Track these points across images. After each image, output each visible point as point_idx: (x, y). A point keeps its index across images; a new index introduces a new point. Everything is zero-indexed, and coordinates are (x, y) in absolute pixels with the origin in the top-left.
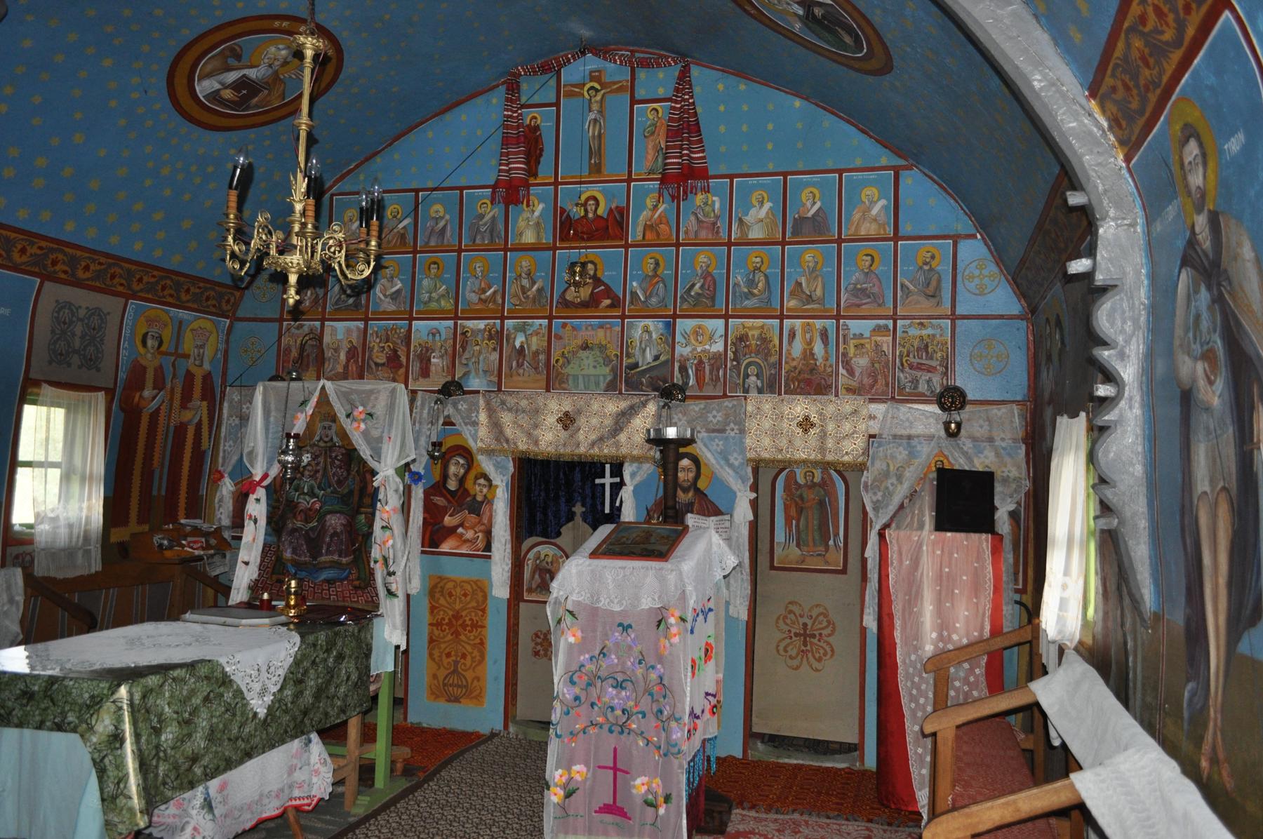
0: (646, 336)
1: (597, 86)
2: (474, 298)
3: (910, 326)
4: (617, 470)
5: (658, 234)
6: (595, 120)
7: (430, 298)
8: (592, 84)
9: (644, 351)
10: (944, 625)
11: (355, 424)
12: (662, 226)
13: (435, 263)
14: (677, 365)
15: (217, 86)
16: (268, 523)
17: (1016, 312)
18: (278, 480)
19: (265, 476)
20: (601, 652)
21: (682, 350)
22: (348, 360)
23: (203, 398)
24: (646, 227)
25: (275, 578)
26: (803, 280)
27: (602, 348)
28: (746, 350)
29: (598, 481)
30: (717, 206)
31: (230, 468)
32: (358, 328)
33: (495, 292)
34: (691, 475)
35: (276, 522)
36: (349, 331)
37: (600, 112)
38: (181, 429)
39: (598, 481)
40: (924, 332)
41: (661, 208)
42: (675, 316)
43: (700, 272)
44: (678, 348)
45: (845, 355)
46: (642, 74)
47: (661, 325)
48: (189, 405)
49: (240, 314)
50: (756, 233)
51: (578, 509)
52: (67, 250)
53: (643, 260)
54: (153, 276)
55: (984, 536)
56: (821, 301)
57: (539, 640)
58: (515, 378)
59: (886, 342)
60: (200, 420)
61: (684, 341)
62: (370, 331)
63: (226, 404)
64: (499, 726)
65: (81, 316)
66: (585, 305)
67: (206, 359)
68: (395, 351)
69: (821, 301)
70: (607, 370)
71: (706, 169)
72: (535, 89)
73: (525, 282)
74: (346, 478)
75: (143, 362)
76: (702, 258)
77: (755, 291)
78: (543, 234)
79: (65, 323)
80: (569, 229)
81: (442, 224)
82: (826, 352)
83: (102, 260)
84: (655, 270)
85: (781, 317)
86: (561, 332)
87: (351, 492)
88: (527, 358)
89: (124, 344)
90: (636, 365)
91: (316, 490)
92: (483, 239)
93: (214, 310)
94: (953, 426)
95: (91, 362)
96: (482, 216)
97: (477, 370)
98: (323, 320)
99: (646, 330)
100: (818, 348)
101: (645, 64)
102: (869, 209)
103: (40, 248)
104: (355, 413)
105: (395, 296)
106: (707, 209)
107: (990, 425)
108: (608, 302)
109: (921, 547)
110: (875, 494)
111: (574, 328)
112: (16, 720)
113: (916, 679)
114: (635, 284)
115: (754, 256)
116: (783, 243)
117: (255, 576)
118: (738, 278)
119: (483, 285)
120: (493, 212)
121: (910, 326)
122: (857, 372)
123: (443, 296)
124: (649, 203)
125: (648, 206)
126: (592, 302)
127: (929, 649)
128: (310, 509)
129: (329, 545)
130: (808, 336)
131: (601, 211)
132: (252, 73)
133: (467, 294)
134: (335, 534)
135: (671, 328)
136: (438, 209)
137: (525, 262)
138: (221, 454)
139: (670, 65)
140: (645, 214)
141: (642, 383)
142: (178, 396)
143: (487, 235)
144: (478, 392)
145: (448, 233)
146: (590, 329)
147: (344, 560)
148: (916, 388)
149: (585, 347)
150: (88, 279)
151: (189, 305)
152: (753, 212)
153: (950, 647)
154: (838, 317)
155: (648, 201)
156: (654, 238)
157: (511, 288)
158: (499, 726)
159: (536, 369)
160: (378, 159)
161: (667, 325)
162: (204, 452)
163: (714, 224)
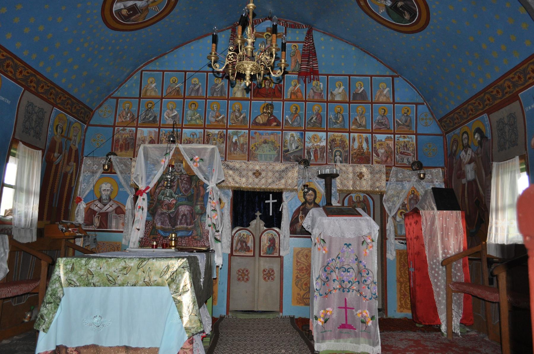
2: (213, 120)
3: (400, 137)
4: (278, 195)
5: (297, 96)
7: (191, 119)
9: (292, 145)
10: (445, 248)
11: (195, 164)
13: (194, 104)
15: (122, 7)
16: (148, 211)
17: (439, 133)
19: (147, 188)
20: (337, 257)
21: (308, 145)
24: (291, 93)
25: (152, 236)
26: (358, 118)
27: (273, 143)
29: (266, 202)
30: (322, 86)
31: (84, 196)
32: (155, 131)
33: (223, 118)
34: (313, 197)
35: (152, 211)
38: (66, 175)
39: (266, 202)
40: (405, 140)
41: (298, 86)
42: (305, 131)
43: (315, 113)
44: (306, 144)
45: (375, 148)
46: (289, 30)
47: (299, 134)
48: (70, 164)
49: (92, 122)
50: (337, 98)
51: (258, 214)
52: (38, 76)
53: (292, 107)
55: (458, 212)
56: (365, 126)
57: (240, 273)
58: (233, 155)
59: (391, 144)
61: (308, 141)
62: (161, 133)
63: (83, 166)
64: (224, 313)
65: (36, 111)
66: (264, 124)
67: (77, 143)
69: (365, 126)
70: (275, 152)
71: (318, 71)
73: (237, 114)
74: (189, 189)
75: (56, 139)
76: (316, 107)
79: (30, 113)
81: (197, 87)
82: (368, 146)
83: (49, 84)
84: (296, 111)
85: (349, 132)
86: (254, 136)
87: (192, 195)
89: (50, 129)
90: (288, 151)
91: (174, 195)
92: (217, 94)
94: (422, 176)
95: (38, 135)
96: (217, 85)
98: (137, 127)
99: (292, 136)
100: (365, 145)
101: (293, 26)
102: (383, 91)
103: (28, 73)
104: (195, 158)
105: (174, 117)
106: (318, 87)
107: (432, 176)
108: (275, 124)
109: (434, 216)
110: (389, 204)
111: (260, 134)
112: (119, 282)
113: (437, 270)
114: (287, 116)
115: (338, 107)
116: (349, 103)
117: (142, 236)
118: (331, 116)
121: (400, 137)
122: (380, 155)
124: (293, 83)
125: (292, 85)
126: (268, 123)
127: (440, 258)
128: (170, 204)
129: (181, 220)
130: (360, 140)
132: (139, 4)
134: (184, 215)
135: (303, 136)
136: (195, 80)
138: (79, 190)
139: (303, 28)
140: (291, 88)
141: (291, 158)
142: (66, 158)
143: (219, 93)
145: (200, 91)
146: (267, 135)
147: (189, 227)
148: (403, 161)
149: (265, 142)
150: (42, 93)
152: (336, 89)
153: (449, 256)
154: (372, 133)
155: (292, 82)
156: (295, 98)
157: (231, 116)
158: (224, 313)
159: (243, 151)
160: (166, 56)
161: (302, 134)
163: (321, 93)
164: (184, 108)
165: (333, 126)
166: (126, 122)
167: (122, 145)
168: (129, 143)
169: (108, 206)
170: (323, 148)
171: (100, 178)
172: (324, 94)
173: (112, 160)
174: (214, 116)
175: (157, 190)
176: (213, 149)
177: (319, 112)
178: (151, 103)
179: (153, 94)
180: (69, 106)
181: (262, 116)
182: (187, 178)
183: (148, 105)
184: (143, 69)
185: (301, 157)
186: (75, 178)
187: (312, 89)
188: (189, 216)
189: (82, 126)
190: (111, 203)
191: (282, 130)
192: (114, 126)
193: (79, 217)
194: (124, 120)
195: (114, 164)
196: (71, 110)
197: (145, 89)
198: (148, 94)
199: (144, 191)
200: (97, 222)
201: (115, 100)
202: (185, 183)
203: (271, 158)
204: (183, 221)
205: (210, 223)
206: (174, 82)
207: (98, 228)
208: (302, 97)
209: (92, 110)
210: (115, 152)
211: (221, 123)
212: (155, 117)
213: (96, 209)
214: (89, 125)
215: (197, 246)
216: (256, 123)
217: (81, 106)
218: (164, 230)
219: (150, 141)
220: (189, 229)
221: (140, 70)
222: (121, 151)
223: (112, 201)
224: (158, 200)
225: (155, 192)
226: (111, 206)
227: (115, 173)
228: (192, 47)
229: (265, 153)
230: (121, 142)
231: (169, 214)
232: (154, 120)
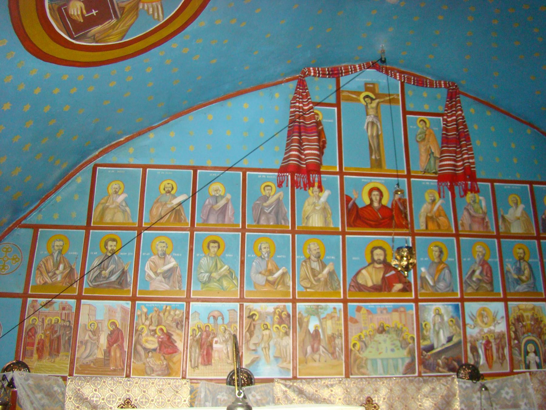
0: (438, 319)
1: (373, 96)
5: (439, 225)
6: (373, 123)
7: (210, 278)
8: (367, 93)
9: (438, 333)
12: (441, 218)
13: (215, 242)
14: (469, 345)
21: (472, 332)
22: (110, 345)
27: (398, 331)
28: (524, 330)
30: (483, 204)
32: (123, 309)
33: (284, 274)
36: (111, 311)
37: (376, 116)
41: (439, 202)
42: (462, 300)
43: (478, 260)
46: (411, 90)
47: (450, 308)
50: (516, 229)
58: (311, 364)
62: (138, 312)
66: (376, 289)
68: (169, 336)
70: (404, 353)
72: (321, 89)
73: (315, 265)
76: (478, 248)
77: (523, 278)
78: (330, 219)
80: (358, 217)
81: (222, 203)
86: (356, 316)
88: (323, 343)
90: (431, 348)
96: (266, 198)
97: (267, 356)
98: (79, 298)
99: (438, 313)
101: (420, 82)
105: (168, 275)
106: (476, 206)
108: (399, 286)
111: (369, 312)
114: (423, 269)
118: (509, 267)
120: (275, 194)
123: (225, 276)
124: (428, 198)
126: (385, 286)
131: (386, 201)
133: (253, 275)
135: (460, 312)
136: (217, 188)
137: (314, 244)
141: (438, 365)
143: (272, 216)
144: (271, 380)
145: (230, 212)
149: (382, 330)
152: (511, 211)
157: (302, 271)
159: (333, 354)
160: (151, 135)
161: (457, 307)
163: (483, 219)
164: (191, 250)
165: (514, 287)
166: (54, 284)
167: (41, 343)
170: (500, 337)
172: (490, 219)
174: (263, 269)
177: (486, 258)
178: (114, 240)
179: (120, 218)
181: (370, 268)
183: (106, 244)
184: (98, 161)
185: (459, 361)
187: (468, 210)
191: (416, 301)
192: (25, 296)
194: (49, 281)
197: (101, 207)
198: (108, 218)
203: (396, 368)
206: (169, 192)
208: (450, 227)
211: (280, 288)
216: (361, 288)
219: (112, 332)
221: (92, 164)
222: (40, 358)
228: (210, 117)
229: (382, 356)
230: (40, 335)
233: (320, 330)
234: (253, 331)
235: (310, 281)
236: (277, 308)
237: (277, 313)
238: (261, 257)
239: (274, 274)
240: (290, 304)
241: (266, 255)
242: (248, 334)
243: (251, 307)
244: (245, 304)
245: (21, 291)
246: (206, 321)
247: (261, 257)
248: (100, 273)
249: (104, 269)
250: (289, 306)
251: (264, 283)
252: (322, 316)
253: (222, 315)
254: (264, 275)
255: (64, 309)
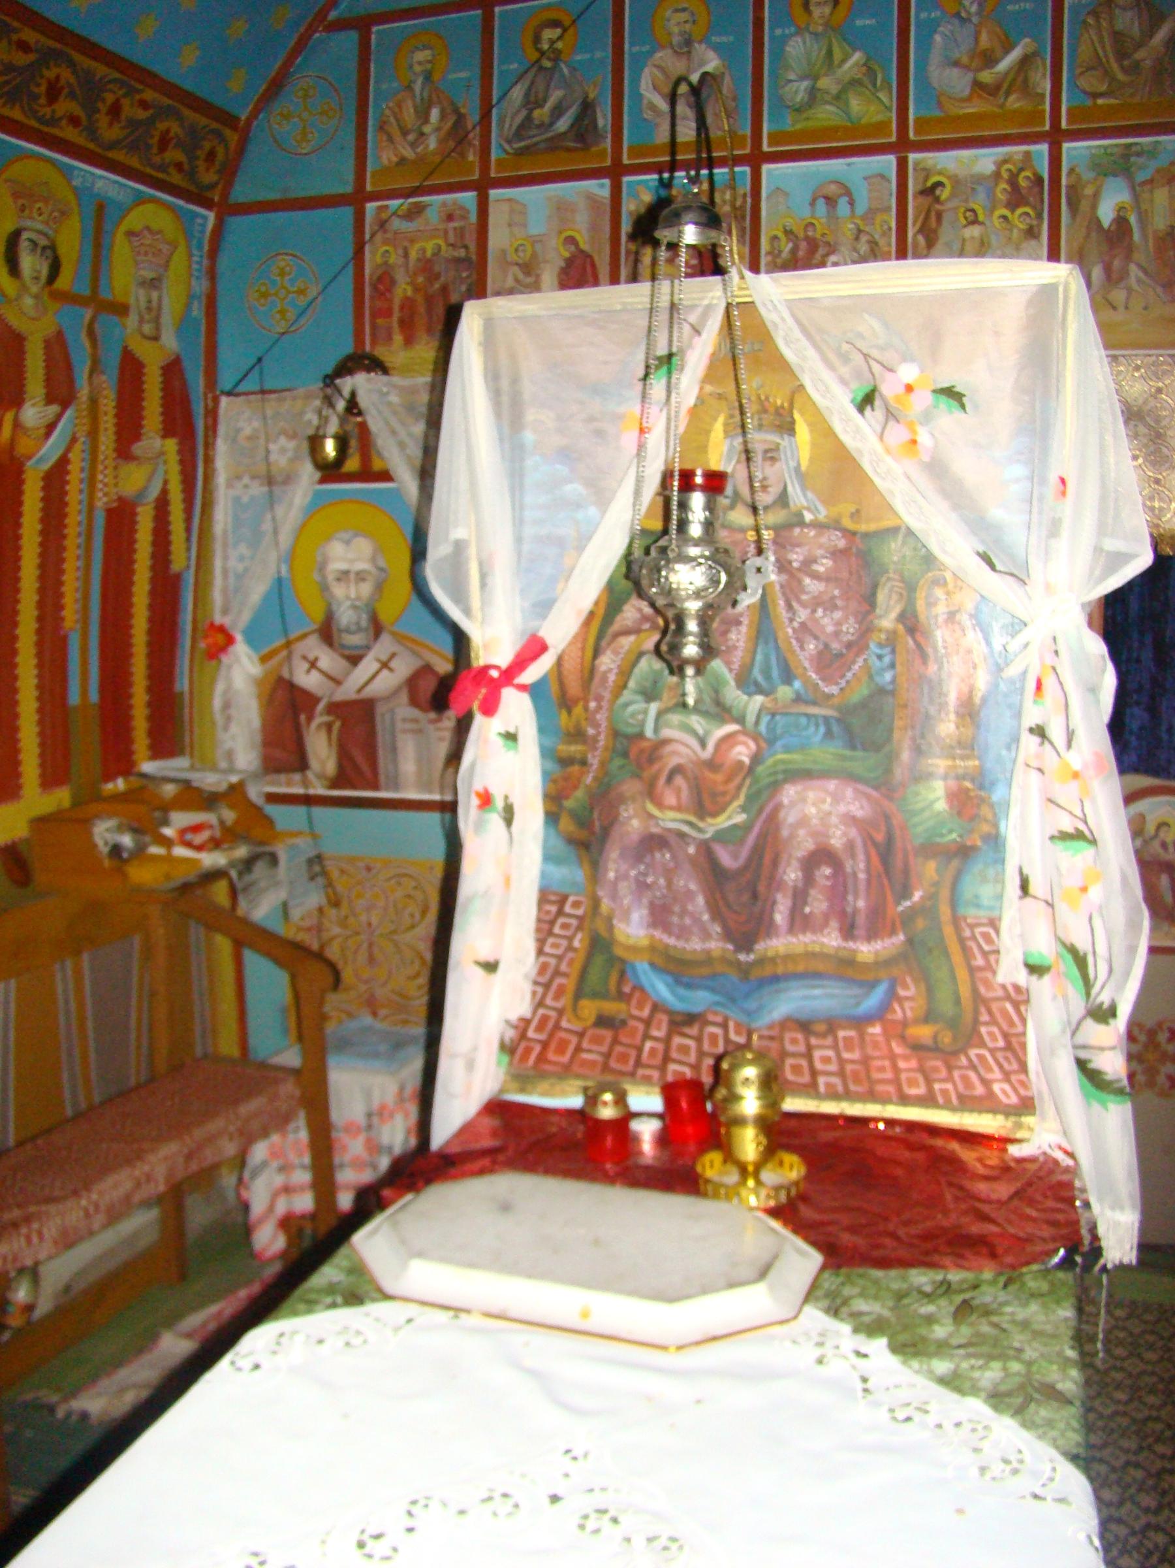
7: (813, 92)
11: (897, 434)
16: (552, 817)
18: (570, 665)
19: (534, 648)
23: (168, 431)
25: (590, 1009)
31: (246, 617)
32: (591, 199)
33: (1025, 61)
35: (582, 821)
36: (562, 209)
38: (121, 518)
48: (137, 449)
49: (241, 192)
54: (24, 47)
60: (164, 492)
63: (221, 447)
67: (167, 320)
74: (857, 646)
91: (733, 695)
93: (176, 178)
98: (482, 187)
104: (889, 389)
117: (522, 1007)
119: (985, 40)
123: (854, 83)
128: (712, 765)
129: (800, 897)
134: (822, 855)
142: (108, 422)
147: (866, 951)
151: (118, 156)
162: (178, 577)
166: (421, 159)
167: (408, 304)
168: (445, 289)
169: (368, 666)
171: (313, 510)
173: (363, 401)
174: (961, 53)
175: (608, 662)
176: (1047, 294)
178: (555, 24)
180: (65, 106)
182: (835, 554)
183: (537, 39)
186: (188, 520)
188: (858, 867)
189: (185, 223)
190: (384, 646)
192: (357, 198)
193: (234, 729)
194: (408, 153)
195: (375, 424)
196: (92, 132)
199: (509, 675)
200: (322, 751)
201: (353, 36)
202: (817, 602)
204: (817, 904)
205: (1044, 948)
207: (335, 783)
209: (229, 120)
210: (381, 352)
211: (1014, 102)
212: (587, 108)
213: (308, 680)
214: (227, 210)
215: (929, 1100)
217: (149, 95)
218: (677, 967)
219: (570, 262)
220: (866, 967)
222: (409, 341)
223: (385, 638)
224: (616, 734)
225: (589, 674)
226: (385, 665)
227: (385, 476)
230: (403, 289)
231: (706, 848)
232: (584, 131)
233: (1133, 220)
234: (935, 231)
235: (1106, 72)
236: (1005, 162)
237: (1005, 175)
238: (957, 15)
239: (997, 62)
240: (1043, 148)
241: (974, 9)
242: (921, 239)
243: (930, 163)
244: (912, 157)
245: (348, 189)
246: (806, 213)
247: (957, 15)
248: (529, 118)
249: (540, 104)
250: (1040, 153)
251: (967, 92)
252: (1141, 177)
253: (848, 193)
254: (967, 68)
255: (450, 218)
